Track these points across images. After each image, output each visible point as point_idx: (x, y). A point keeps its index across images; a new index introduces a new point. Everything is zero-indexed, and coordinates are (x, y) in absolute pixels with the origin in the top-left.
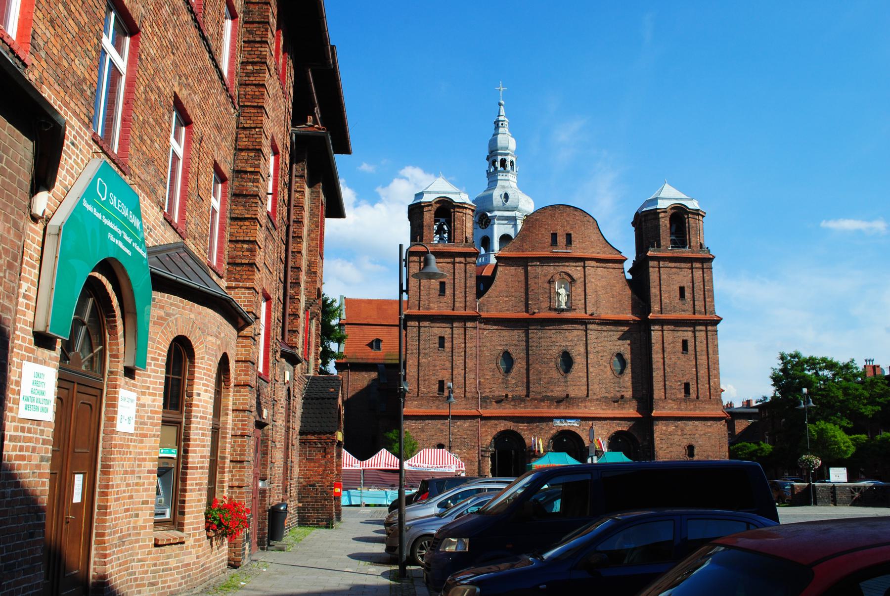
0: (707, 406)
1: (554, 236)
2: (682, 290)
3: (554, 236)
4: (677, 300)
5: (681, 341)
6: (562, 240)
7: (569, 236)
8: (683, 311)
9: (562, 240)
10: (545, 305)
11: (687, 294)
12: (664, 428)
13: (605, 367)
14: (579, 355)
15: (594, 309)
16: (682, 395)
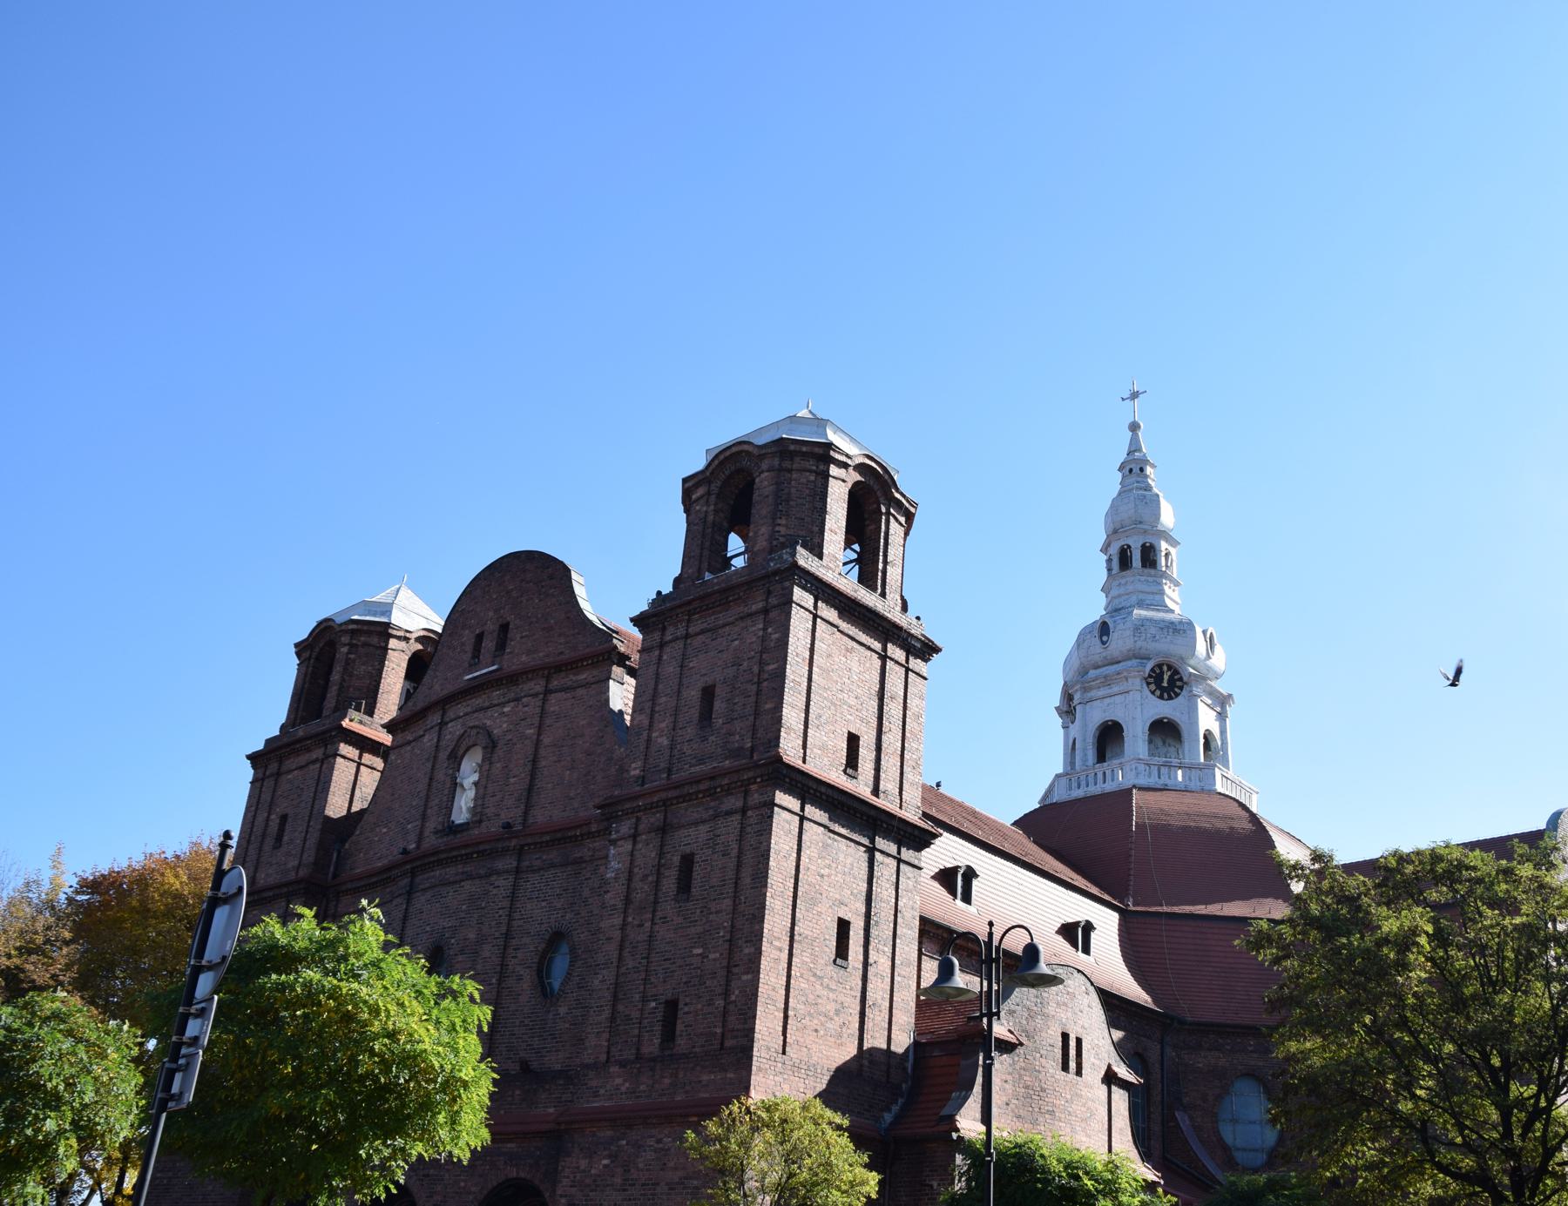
0: (705, 1078)
1: (480, 638)
2: (708, 693)
3: (480, 638)
4: (690, 731)
5: (676, 859)
6: (489, 644)
7: (504, 628)
8: (701, 761)
9: (489, 644)
10: (431, 825)
11: (719, 705)
12: (583, 1164)
13: (520, 979)
14: (462, 952)
15: (520, 811)
16: (652, 1046)
